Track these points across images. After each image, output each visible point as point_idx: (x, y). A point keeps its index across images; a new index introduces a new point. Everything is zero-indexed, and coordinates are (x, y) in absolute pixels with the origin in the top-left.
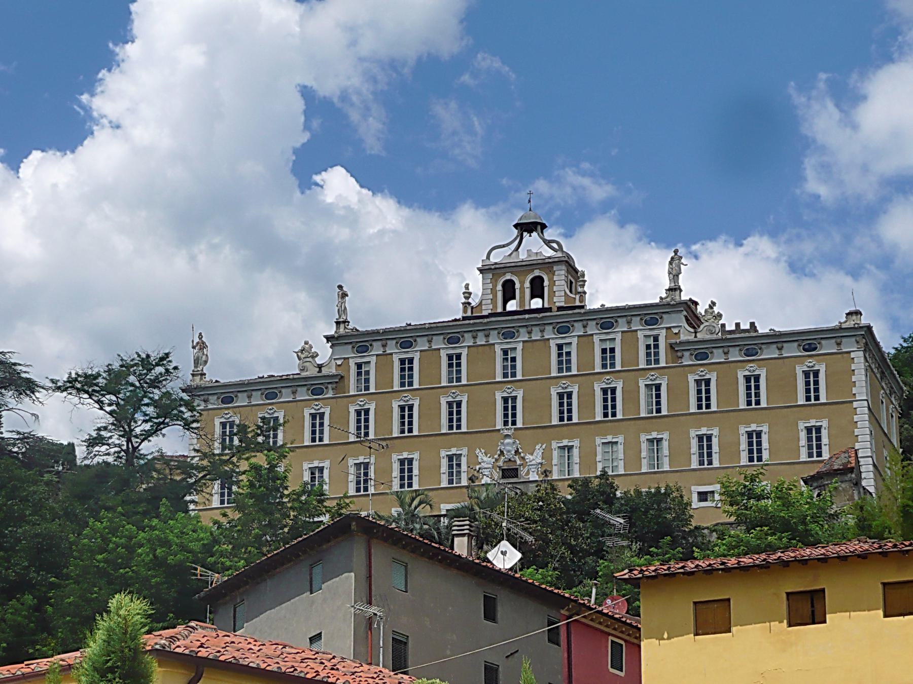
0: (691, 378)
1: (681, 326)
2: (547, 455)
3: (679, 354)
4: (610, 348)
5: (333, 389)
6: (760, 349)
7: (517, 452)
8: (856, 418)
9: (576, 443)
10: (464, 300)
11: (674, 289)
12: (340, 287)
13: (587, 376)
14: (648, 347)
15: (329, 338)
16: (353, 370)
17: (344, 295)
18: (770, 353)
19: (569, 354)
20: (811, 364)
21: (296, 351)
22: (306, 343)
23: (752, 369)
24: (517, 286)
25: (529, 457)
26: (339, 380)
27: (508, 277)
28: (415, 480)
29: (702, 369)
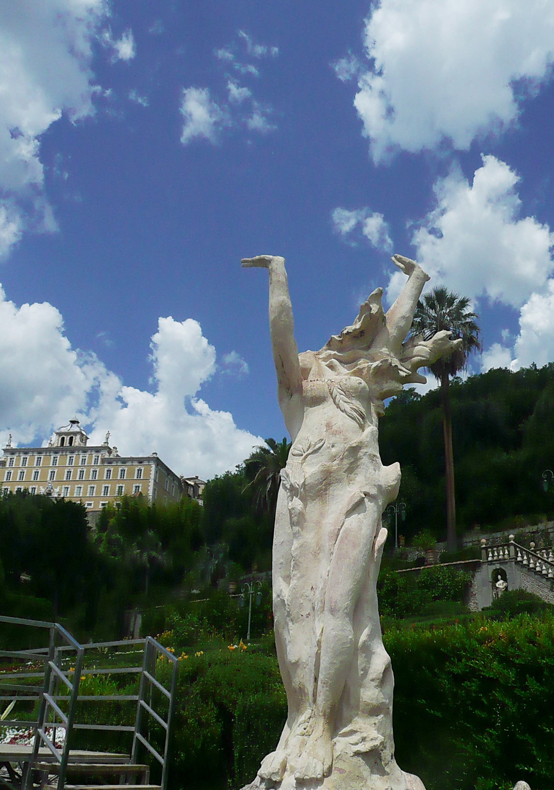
0: (106, 469)
2: (61, 490)
7: (52, 488)
8: (150, 484)
9: (69, 486)
12: (10, 435)
14: (95, 459)
15: (3, 450)
16: (9, 460)
17: (11, 437)
18: (129, 463)
19: (72, 460)
24: (65, 439)
25: (55, 490)
27: (63, 436)
28: (108, 493)
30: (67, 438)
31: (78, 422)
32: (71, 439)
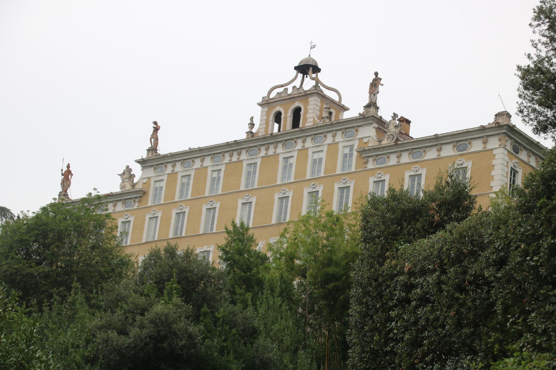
1: (370, 137)
3: (365, 160)
4: (319, 159)
5: (138, 202)
6: (424, 152)
10: (248, 130)
11: (372, 105)
12: (155, 123)
13: (300, 182)
14: (345, 156)
15: (142, 162)
18: (432, 154)
19: (291, 165)
20: (460, 162)
21: (120, 174)
22: (128, 167)
23: (415, 169)
24: (283, 116)
26: (141, 194)
27: (278, 109)
29: (379, 172)
30: (286, 113)
31: (316, 70)
32: (297, 113)
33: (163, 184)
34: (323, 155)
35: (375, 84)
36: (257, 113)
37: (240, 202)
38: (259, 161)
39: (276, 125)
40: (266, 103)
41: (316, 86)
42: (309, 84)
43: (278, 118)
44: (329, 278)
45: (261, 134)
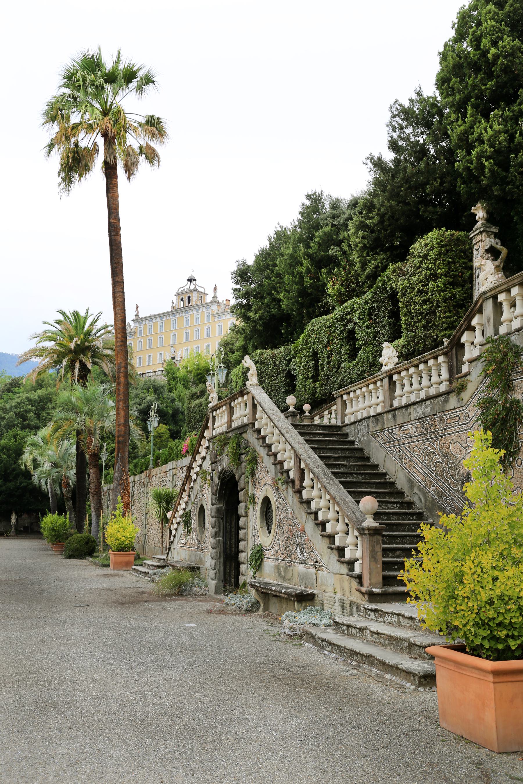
0: (217, 325)
11: (215, 297)
15: (133, 321)
27: (182, 297)
31: (195, 280)
32: (189, 297)
33: (142, 329)
34: (199, 316)
35: (215, 289)
36: (174, 298)
37: (171, 334)
38: (177, 319)
39: (182, 302)
40: (177, 295)
41: (195, 288)
42: (192, 287)
43: (182, 299)
44: (198, 374)
45: (177, 307)
